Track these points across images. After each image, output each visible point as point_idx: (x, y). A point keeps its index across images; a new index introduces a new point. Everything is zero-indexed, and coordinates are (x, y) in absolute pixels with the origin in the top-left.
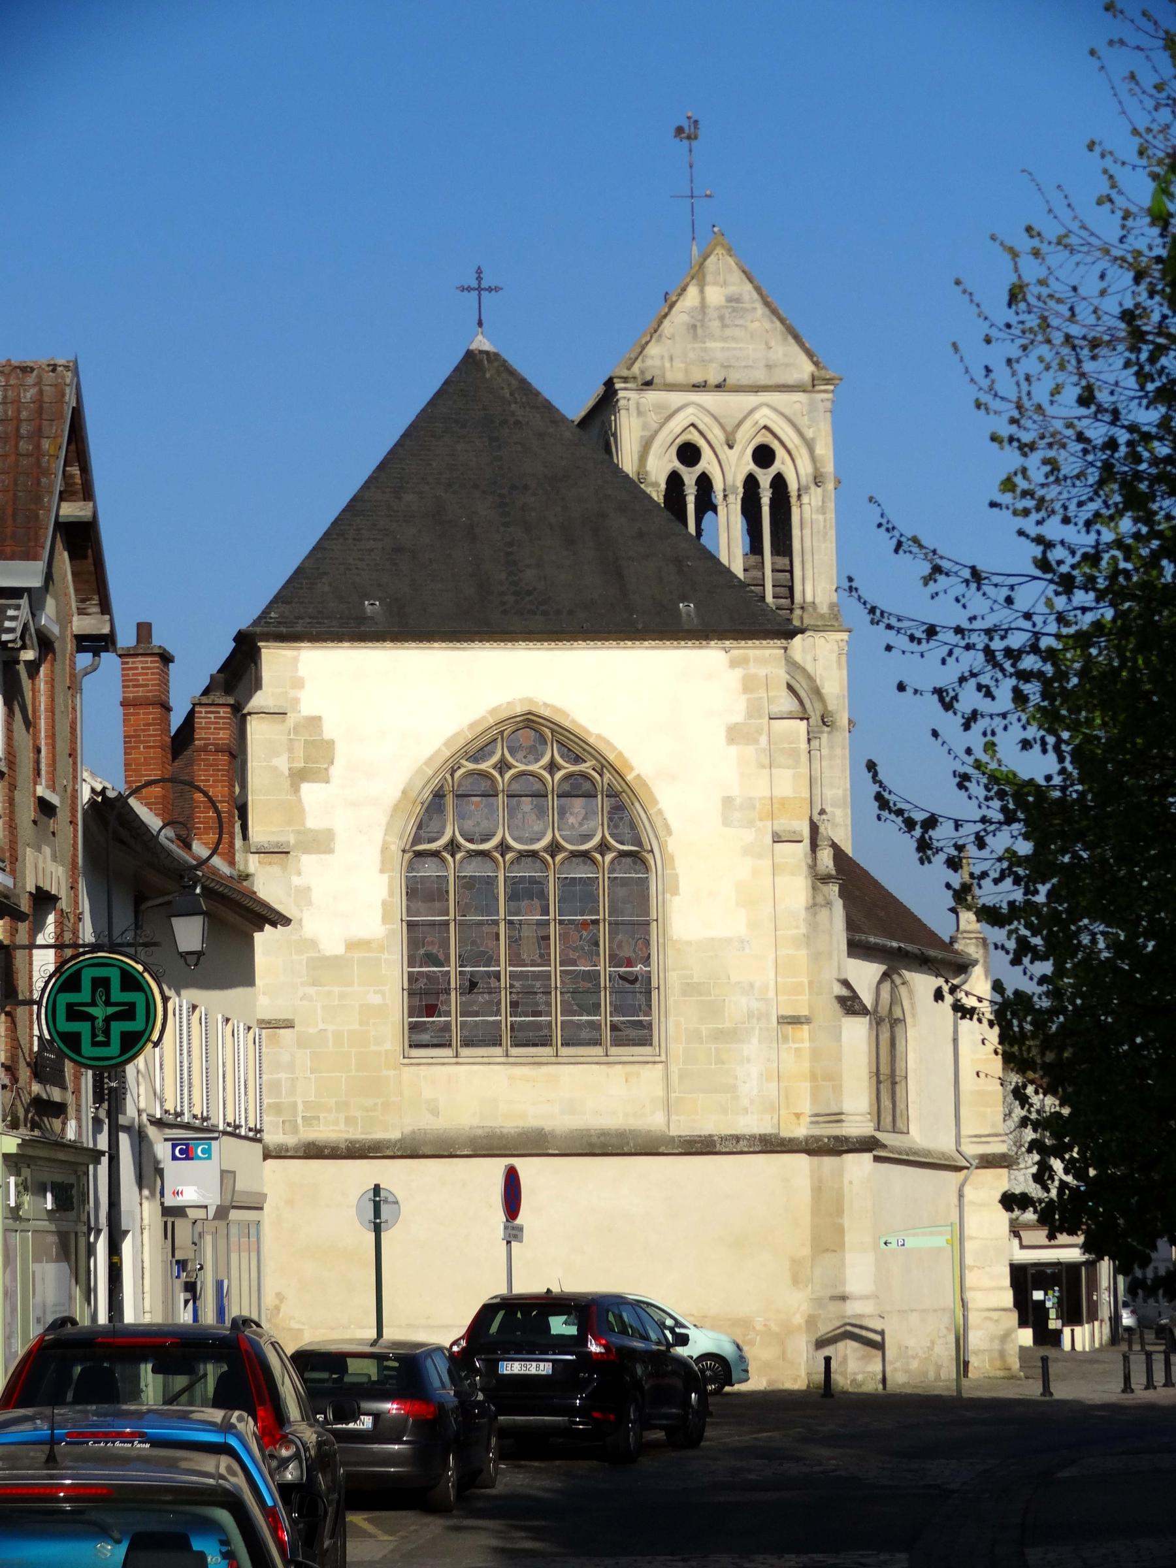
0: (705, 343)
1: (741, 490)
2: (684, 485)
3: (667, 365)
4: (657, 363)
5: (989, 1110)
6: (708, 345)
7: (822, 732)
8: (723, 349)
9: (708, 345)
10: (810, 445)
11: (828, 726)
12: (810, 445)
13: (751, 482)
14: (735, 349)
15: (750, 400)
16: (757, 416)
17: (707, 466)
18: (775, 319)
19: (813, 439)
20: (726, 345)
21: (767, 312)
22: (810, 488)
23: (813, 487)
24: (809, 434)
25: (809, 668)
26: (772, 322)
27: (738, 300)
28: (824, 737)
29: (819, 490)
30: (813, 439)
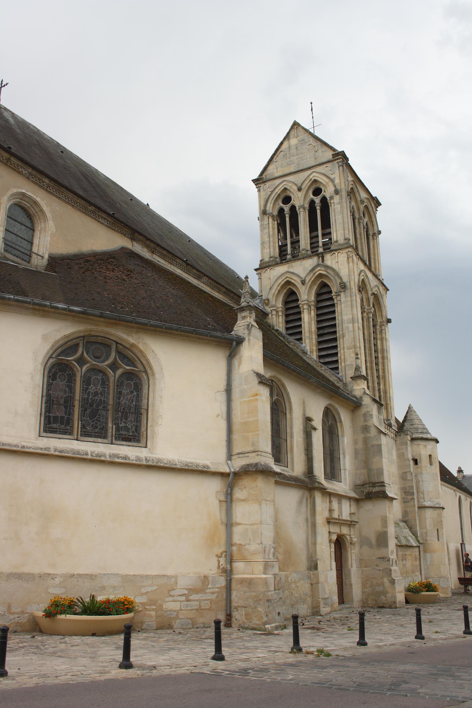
0: (290, 158)
1: (307, 206)
2: (285, 211)
3: (275, 171)
4: (271, 171)
5: (251, 434)
6: (291, 159)
7: (341, 292)
8: (297, 159)
9: (291, 159)
10: (332, 181)
11: (343, 288)
12: (332, 181)
13: (312, 203)
14: (302, 157)
15: (309, 172)
16: (311, 177)
17: (293, 202)
18: (317, 141)
19: (334, 178)
20: (298, 157)
21: (314, 139)
22: (333, 196)
23: (334, 195)
24: (332, 177)
25: (334, 266)
26: (317, 142)
27: (303, 140)
28: (342, 294)
29: (338, 196)
30: (334, 178)
